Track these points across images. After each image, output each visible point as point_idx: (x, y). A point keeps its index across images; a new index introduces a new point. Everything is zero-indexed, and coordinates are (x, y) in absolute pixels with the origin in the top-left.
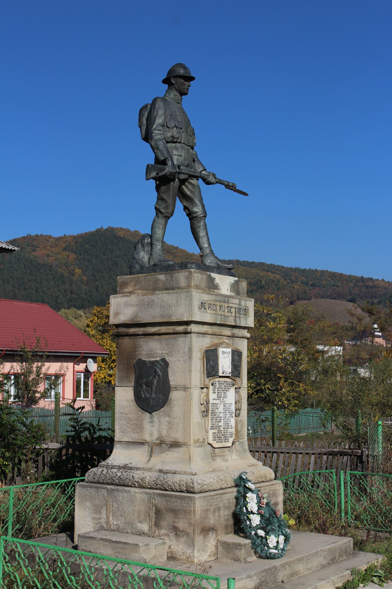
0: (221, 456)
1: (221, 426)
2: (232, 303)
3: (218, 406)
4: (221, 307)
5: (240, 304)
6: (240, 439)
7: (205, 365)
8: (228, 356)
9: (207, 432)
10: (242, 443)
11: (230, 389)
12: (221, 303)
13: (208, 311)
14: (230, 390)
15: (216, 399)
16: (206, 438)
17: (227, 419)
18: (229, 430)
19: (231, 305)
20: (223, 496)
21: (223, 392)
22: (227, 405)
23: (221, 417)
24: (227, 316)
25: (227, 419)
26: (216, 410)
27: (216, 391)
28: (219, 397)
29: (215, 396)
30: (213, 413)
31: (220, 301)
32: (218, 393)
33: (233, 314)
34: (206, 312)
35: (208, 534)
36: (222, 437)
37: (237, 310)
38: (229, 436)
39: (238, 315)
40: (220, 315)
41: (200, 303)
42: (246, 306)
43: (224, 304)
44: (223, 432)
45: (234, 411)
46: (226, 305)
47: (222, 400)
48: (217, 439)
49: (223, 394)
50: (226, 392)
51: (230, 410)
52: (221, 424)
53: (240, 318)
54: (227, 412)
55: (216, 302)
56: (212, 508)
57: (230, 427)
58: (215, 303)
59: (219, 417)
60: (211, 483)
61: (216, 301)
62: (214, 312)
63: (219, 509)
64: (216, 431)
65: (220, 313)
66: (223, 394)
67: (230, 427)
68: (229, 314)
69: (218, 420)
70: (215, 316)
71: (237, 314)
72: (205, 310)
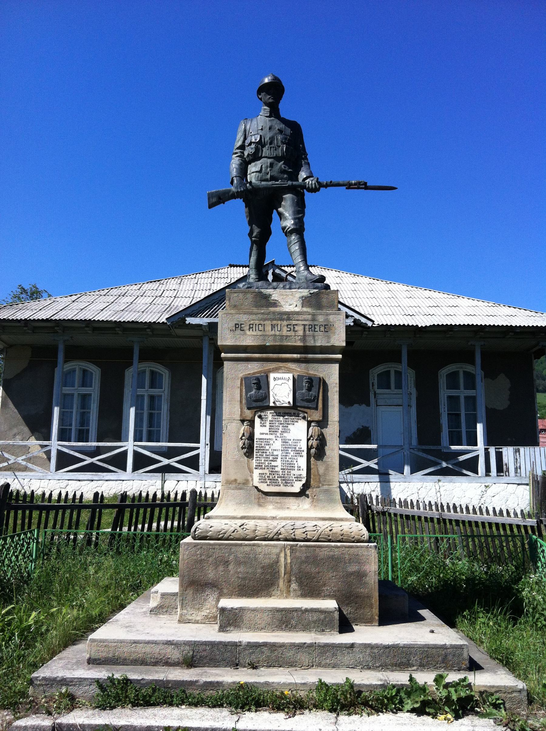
0: (277, 503)
1: (277, 466)
2: (297, 320)
3: (271, 442)
4: (273, 326)
5: (313, 320)
6: (323, 485)
7: (244, 394)
8: (287, 382)
9: (251, 472)
10: (327, 491)
11: (297, 422)
12: (274, 322)
13: (248, 333)
14: (296, 423)
15: (267, 434)
16: (250, 479)
17: (291, 458)
18: (296, 472)
19: (294, 322)
20: (237, 548)
21: (281, 426)
22: (290, 442)
23: (277, 455)
24: (287, 336)
25: (291, 458)
26: (267, 447)
27: (268, 424)
28: (272, 431)
29: (266, 430)
30: (262, 450)
31: (272, 320)
32: (270, 426)
33: (301, 333)
34: (245, 334)
35: (203, 591)
36: (279, 479)
37: (307, 327)
38: (294, 479)
39: (311, 333)
40: (271, 335)
41: (234, 325)
42: (327, 320)
43: (279, 322)
44: (281, 473)
45: (305, 448)
46: (285, 323)
47: (278, 434)
48: (268, 481)
49: (281, 428)
50: (289, 425)
51: (295, 448)
52: (279, 463)
53: (314, 337)
54: (290, 450)
55: (264, 321)
56: (211, 559)
57: (296, 468)
58: (262, 322)
59: (273, 455)
60: (224, 531)
61: (265, 320)
62: (260, 333)
63: (226, 563)
64: (266, 471)
65: (273, 332)
66: (281, 428)
67: (296, 468)
68: (292, 333)
69: (271, 459)
70: (261, 338)
71: (307, 332)
72: (242, 332)
